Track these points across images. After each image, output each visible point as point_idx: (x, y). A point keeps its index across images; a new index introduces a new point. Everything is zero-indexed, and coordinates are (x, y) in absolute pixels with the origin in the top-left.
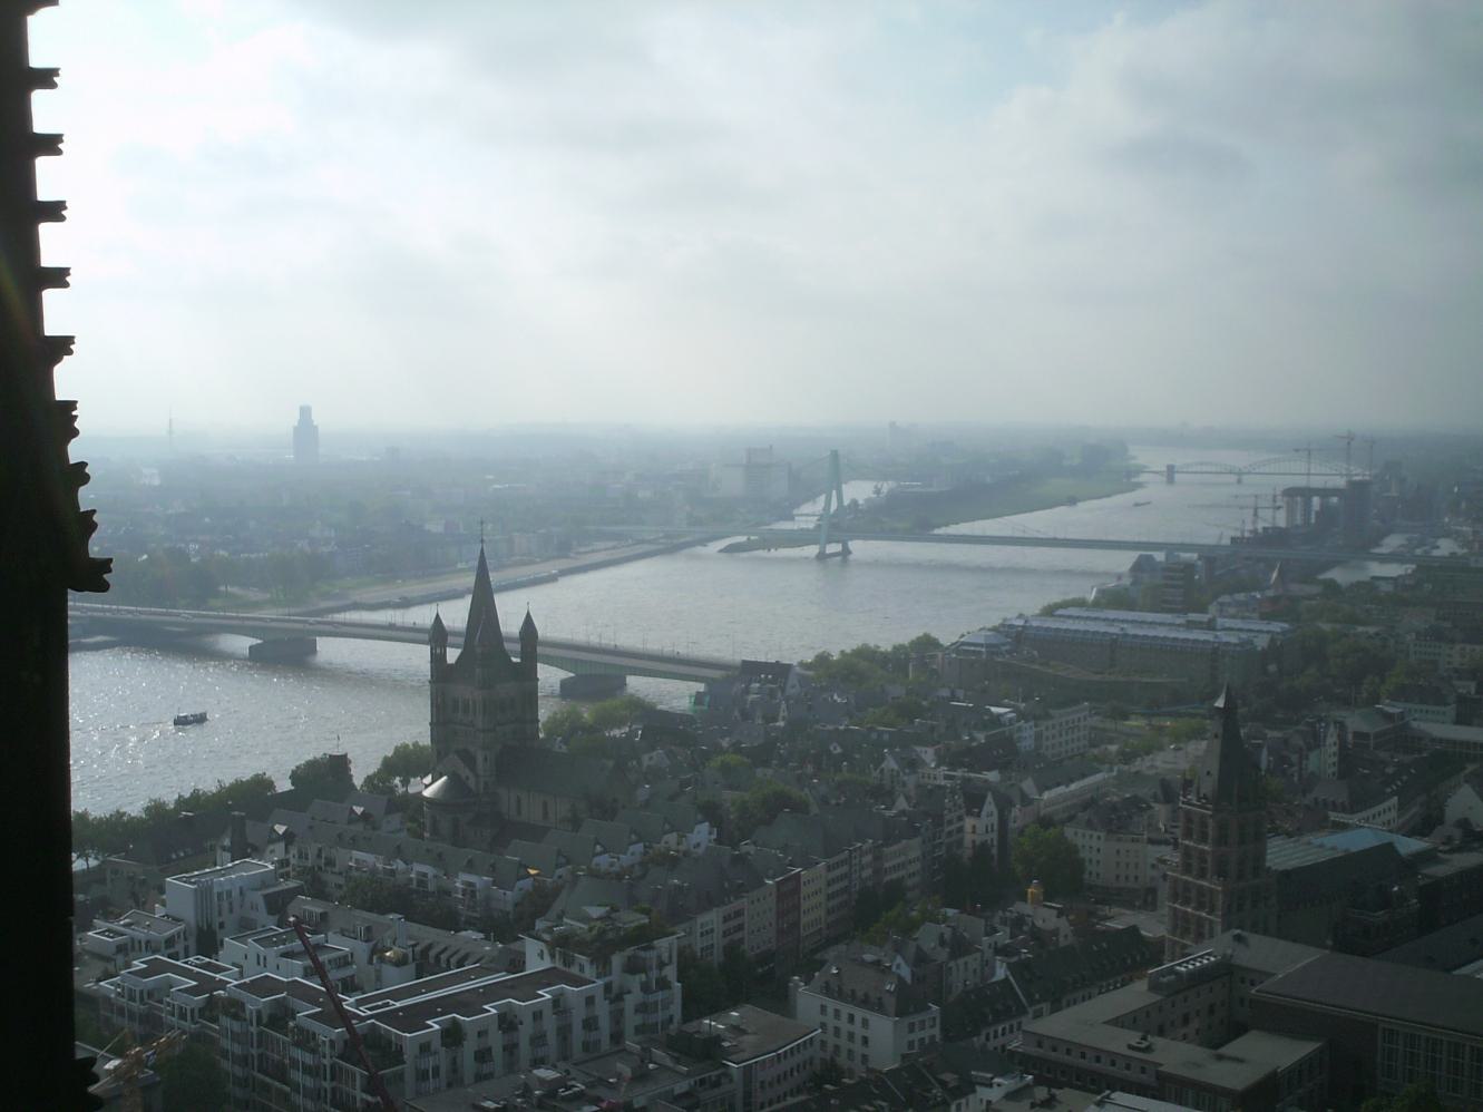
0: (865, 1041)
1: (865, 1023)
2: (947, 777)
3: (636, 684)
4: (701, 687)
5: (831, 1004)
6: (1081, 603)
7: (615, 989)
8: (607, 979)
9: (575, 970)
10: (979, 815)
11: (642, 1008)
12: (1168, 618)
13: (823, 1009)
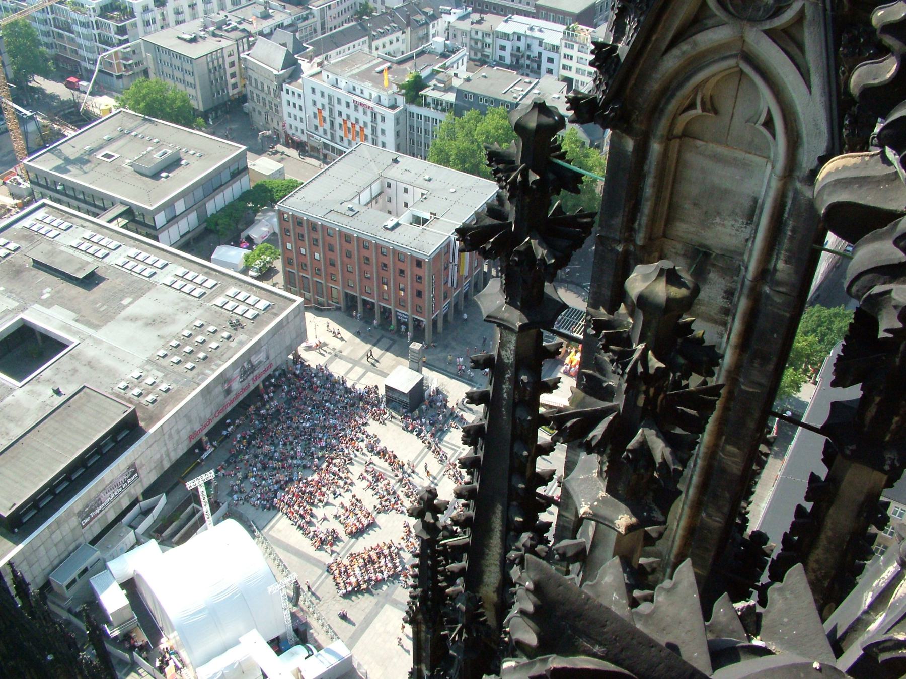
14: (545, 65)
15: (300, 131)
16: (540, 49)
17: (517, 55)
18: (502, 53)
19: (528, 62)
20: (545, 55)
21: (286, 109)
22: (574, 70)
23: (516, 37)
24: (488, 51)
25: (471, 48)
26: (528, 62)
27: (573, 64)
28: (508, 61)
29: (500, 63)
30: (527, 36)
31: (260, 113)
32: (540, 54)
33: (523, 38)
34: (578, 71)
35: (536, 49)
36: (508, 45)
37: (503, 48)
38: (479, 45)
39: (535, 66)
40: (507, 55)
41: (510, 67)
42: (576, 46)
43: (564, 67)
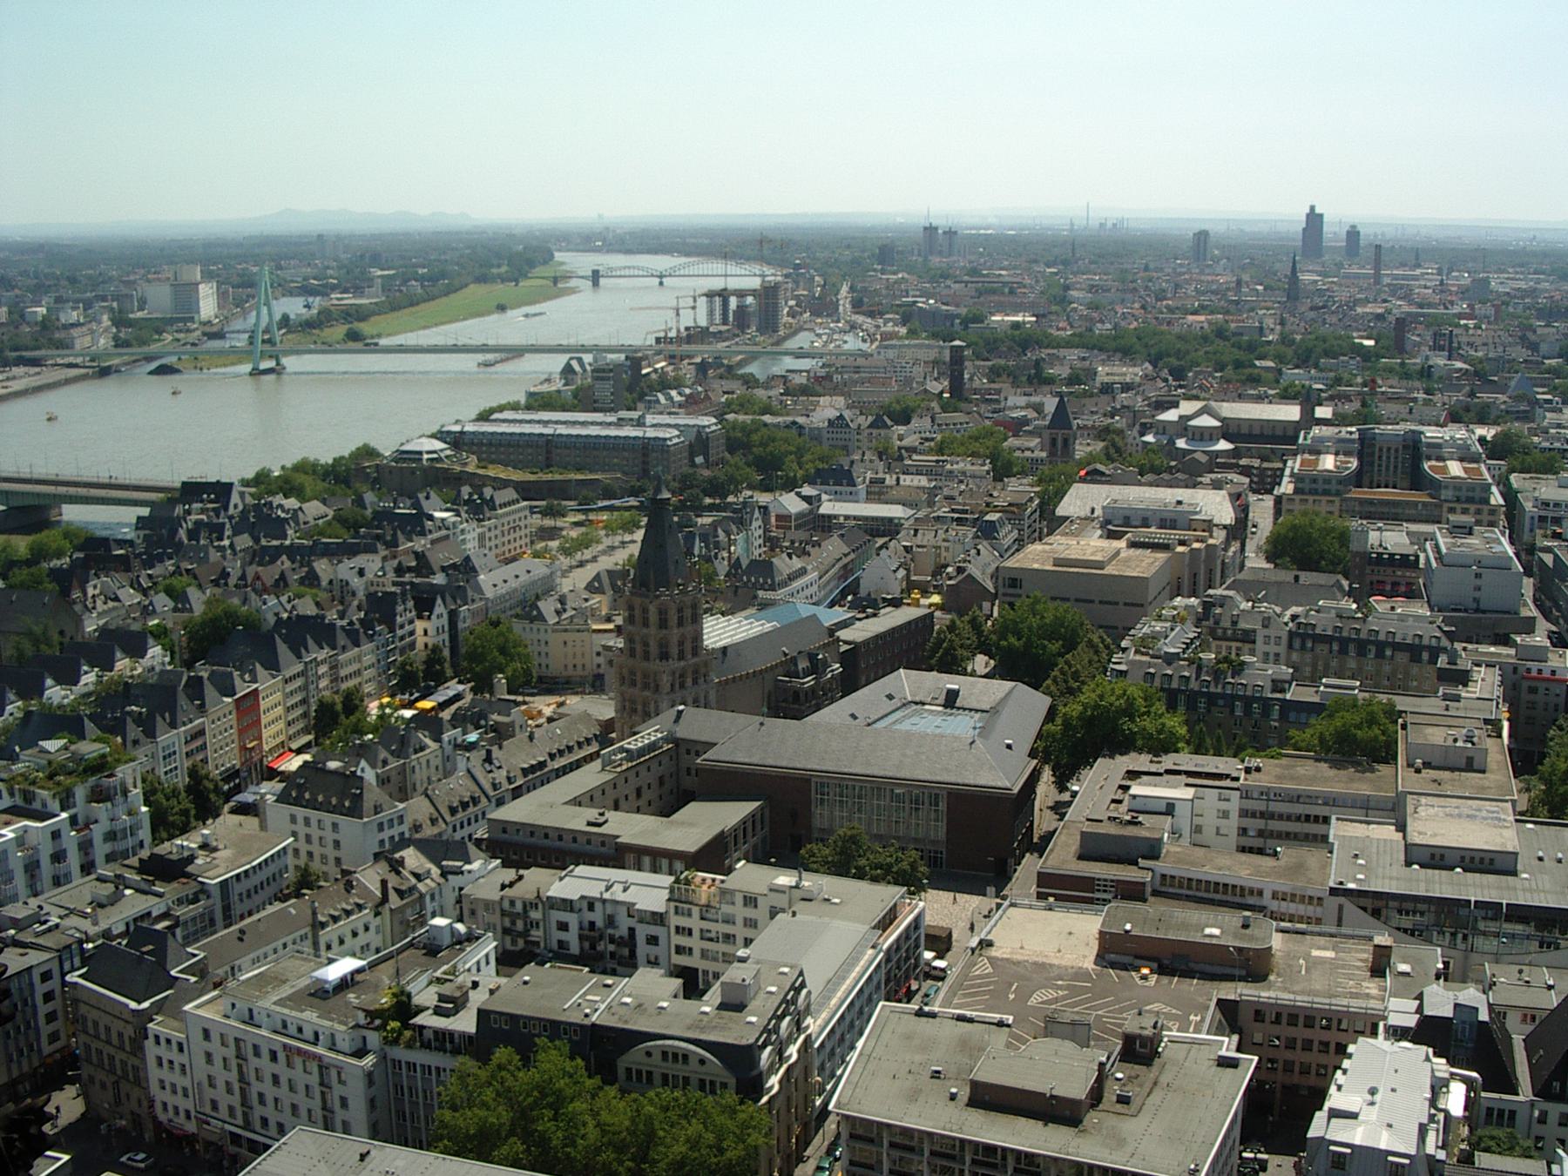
0: (337, 844)
1: (335, 826)
2: (395, 584)
3: (72, 513)
4: (145, 512)
5: (300, 812)
6: (515, 407)
7: (81, 820)
8: (73, 811)
9: (37, 805)
10: (429, 618)
11: (111, 836)
12: (598, 417)
13: (293, 819)
14: (642, 949)
15: (182, 1114)
16: (632, 922)
17: (590, 933)
18: (563, 936)
19: (611, 948)
20: (642, 932)
21: (154, 1073)
22: (697, 953)
23: (585, 905)
24: (536, 934)
25: (506, 931)
26: (611, 948)
27: (694, 942)
28: (575, 949)
29: (561, 955)
30: (604, 901)
31: (103, 1086)
32: (632, 930)
33: (598, 906)
34: (704, 954)
35: (624, 923)
36: (572, 919)
37: (563, 927)
38: (520, 925)
39: (626, 952)
40: (572, 938)
41: (578, 960)
42: (695, 911)
43: (680, 950)
